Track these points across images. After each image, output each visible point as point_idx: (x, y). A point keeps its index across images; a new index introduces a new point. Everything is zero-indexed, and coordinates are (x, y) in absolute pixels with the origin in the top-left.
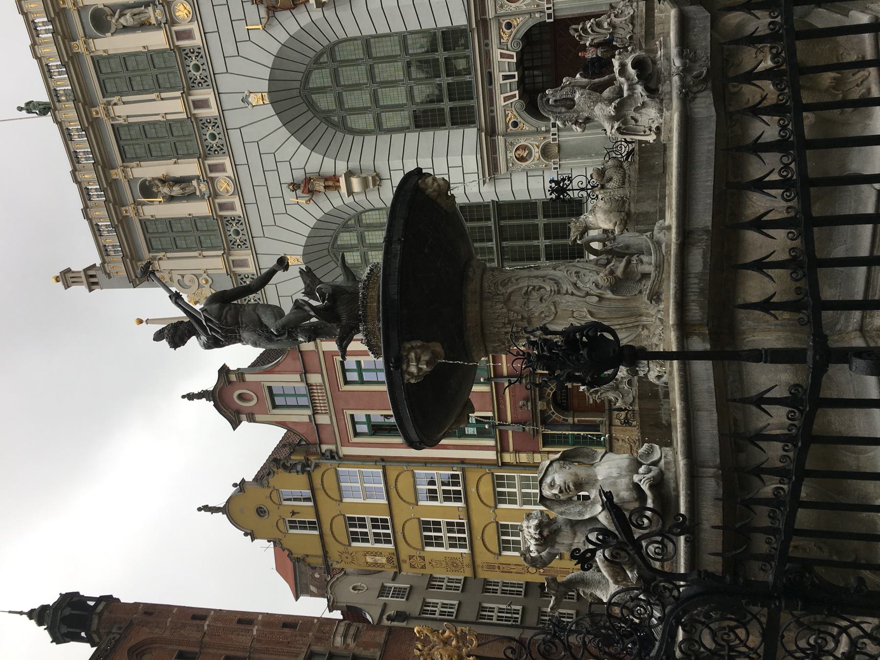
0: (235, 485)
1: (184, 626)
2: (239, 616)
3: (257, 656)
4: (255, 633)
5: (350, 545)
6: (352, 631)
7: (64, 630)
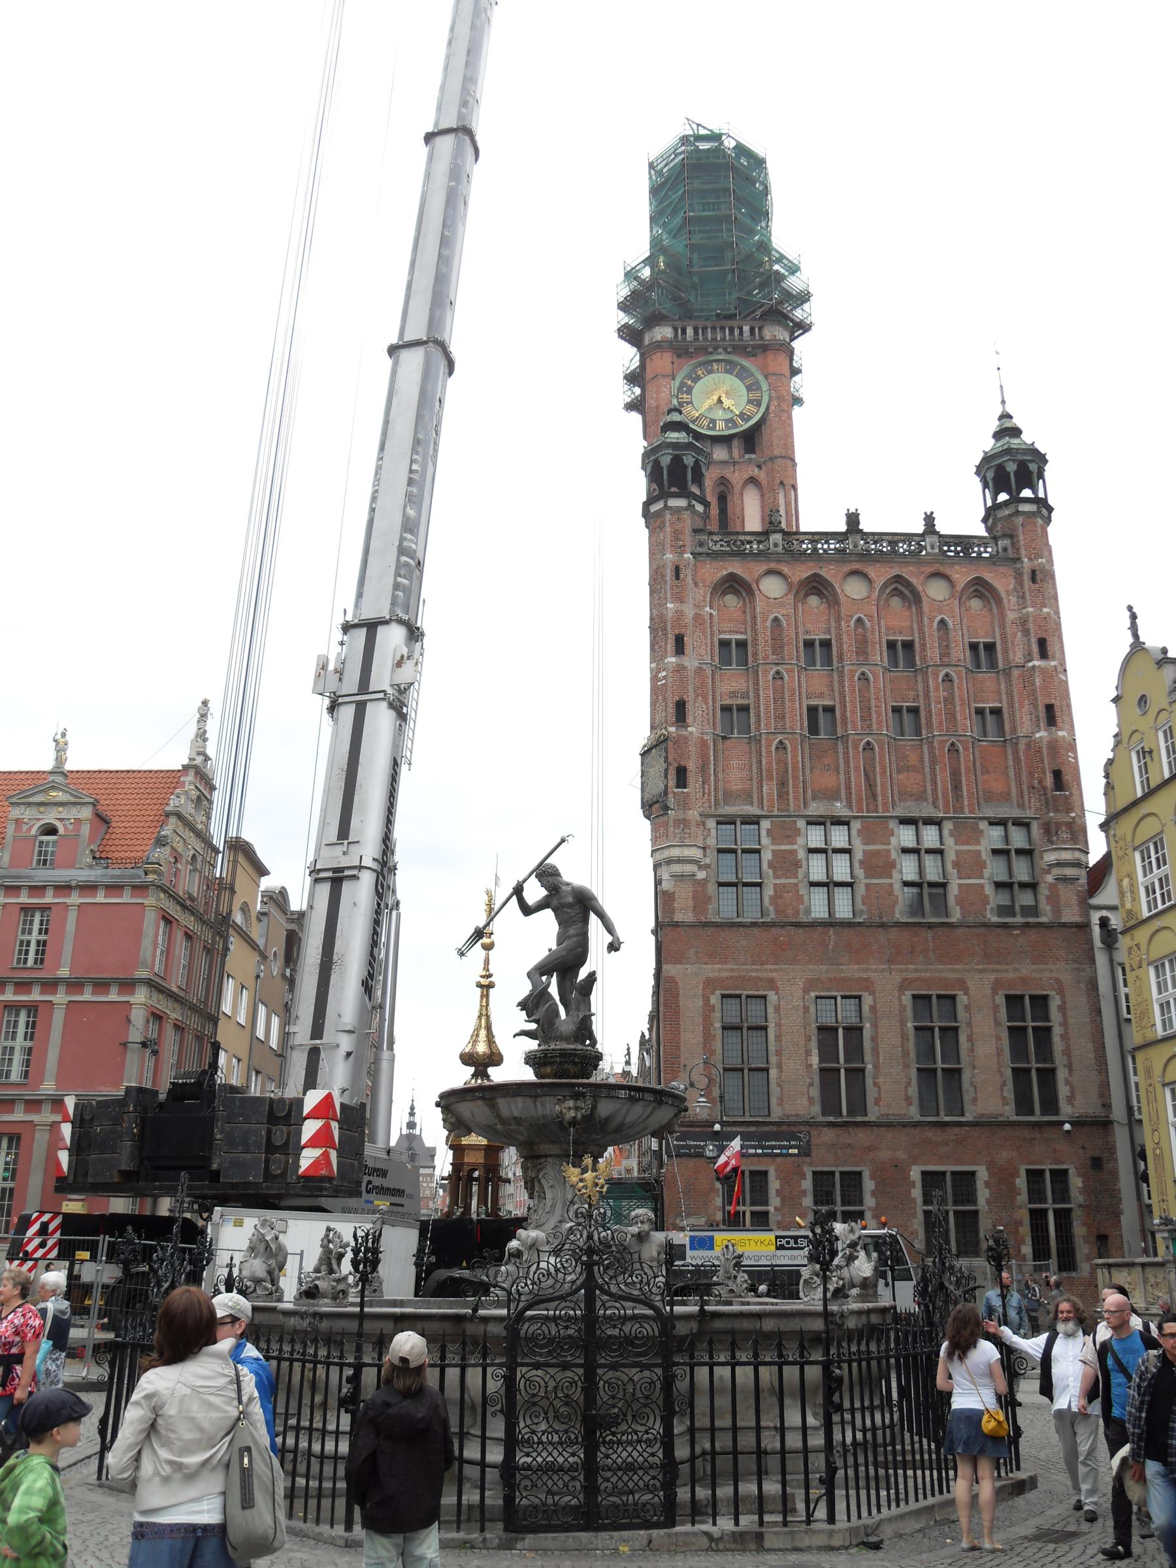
0: (1164, 651)
1: (1026, 632)
2: (1057, 703)
3: (1009, 751)
4: (1038, 735)
5: (1135, 849)
6: (1069, 872)
7: (990, 475)
